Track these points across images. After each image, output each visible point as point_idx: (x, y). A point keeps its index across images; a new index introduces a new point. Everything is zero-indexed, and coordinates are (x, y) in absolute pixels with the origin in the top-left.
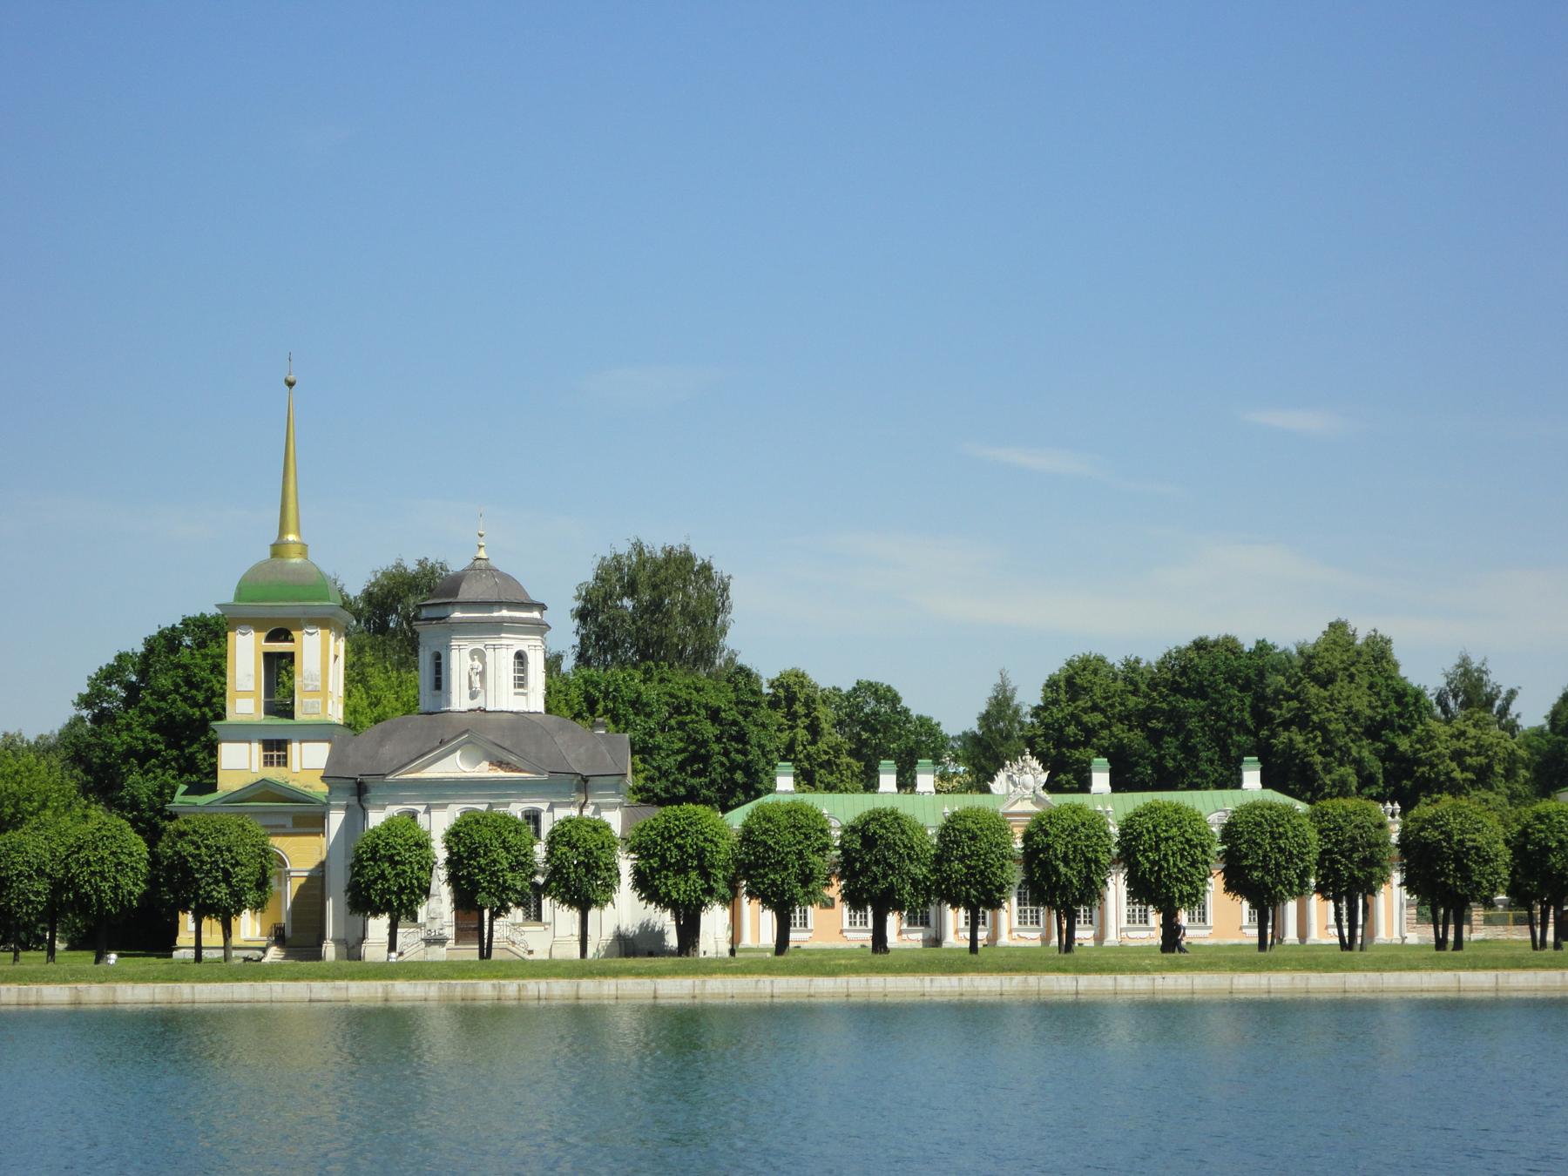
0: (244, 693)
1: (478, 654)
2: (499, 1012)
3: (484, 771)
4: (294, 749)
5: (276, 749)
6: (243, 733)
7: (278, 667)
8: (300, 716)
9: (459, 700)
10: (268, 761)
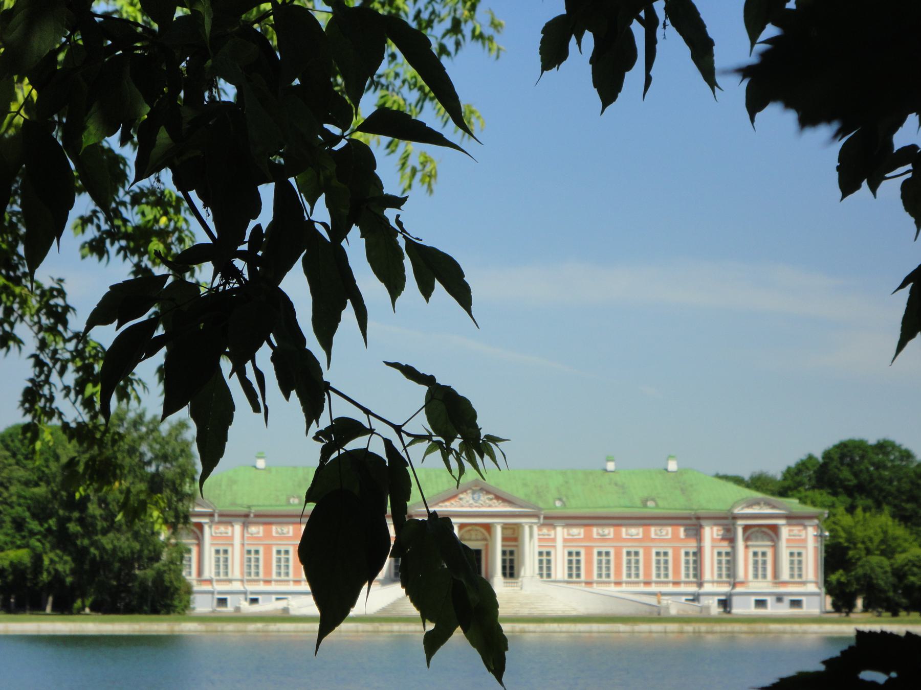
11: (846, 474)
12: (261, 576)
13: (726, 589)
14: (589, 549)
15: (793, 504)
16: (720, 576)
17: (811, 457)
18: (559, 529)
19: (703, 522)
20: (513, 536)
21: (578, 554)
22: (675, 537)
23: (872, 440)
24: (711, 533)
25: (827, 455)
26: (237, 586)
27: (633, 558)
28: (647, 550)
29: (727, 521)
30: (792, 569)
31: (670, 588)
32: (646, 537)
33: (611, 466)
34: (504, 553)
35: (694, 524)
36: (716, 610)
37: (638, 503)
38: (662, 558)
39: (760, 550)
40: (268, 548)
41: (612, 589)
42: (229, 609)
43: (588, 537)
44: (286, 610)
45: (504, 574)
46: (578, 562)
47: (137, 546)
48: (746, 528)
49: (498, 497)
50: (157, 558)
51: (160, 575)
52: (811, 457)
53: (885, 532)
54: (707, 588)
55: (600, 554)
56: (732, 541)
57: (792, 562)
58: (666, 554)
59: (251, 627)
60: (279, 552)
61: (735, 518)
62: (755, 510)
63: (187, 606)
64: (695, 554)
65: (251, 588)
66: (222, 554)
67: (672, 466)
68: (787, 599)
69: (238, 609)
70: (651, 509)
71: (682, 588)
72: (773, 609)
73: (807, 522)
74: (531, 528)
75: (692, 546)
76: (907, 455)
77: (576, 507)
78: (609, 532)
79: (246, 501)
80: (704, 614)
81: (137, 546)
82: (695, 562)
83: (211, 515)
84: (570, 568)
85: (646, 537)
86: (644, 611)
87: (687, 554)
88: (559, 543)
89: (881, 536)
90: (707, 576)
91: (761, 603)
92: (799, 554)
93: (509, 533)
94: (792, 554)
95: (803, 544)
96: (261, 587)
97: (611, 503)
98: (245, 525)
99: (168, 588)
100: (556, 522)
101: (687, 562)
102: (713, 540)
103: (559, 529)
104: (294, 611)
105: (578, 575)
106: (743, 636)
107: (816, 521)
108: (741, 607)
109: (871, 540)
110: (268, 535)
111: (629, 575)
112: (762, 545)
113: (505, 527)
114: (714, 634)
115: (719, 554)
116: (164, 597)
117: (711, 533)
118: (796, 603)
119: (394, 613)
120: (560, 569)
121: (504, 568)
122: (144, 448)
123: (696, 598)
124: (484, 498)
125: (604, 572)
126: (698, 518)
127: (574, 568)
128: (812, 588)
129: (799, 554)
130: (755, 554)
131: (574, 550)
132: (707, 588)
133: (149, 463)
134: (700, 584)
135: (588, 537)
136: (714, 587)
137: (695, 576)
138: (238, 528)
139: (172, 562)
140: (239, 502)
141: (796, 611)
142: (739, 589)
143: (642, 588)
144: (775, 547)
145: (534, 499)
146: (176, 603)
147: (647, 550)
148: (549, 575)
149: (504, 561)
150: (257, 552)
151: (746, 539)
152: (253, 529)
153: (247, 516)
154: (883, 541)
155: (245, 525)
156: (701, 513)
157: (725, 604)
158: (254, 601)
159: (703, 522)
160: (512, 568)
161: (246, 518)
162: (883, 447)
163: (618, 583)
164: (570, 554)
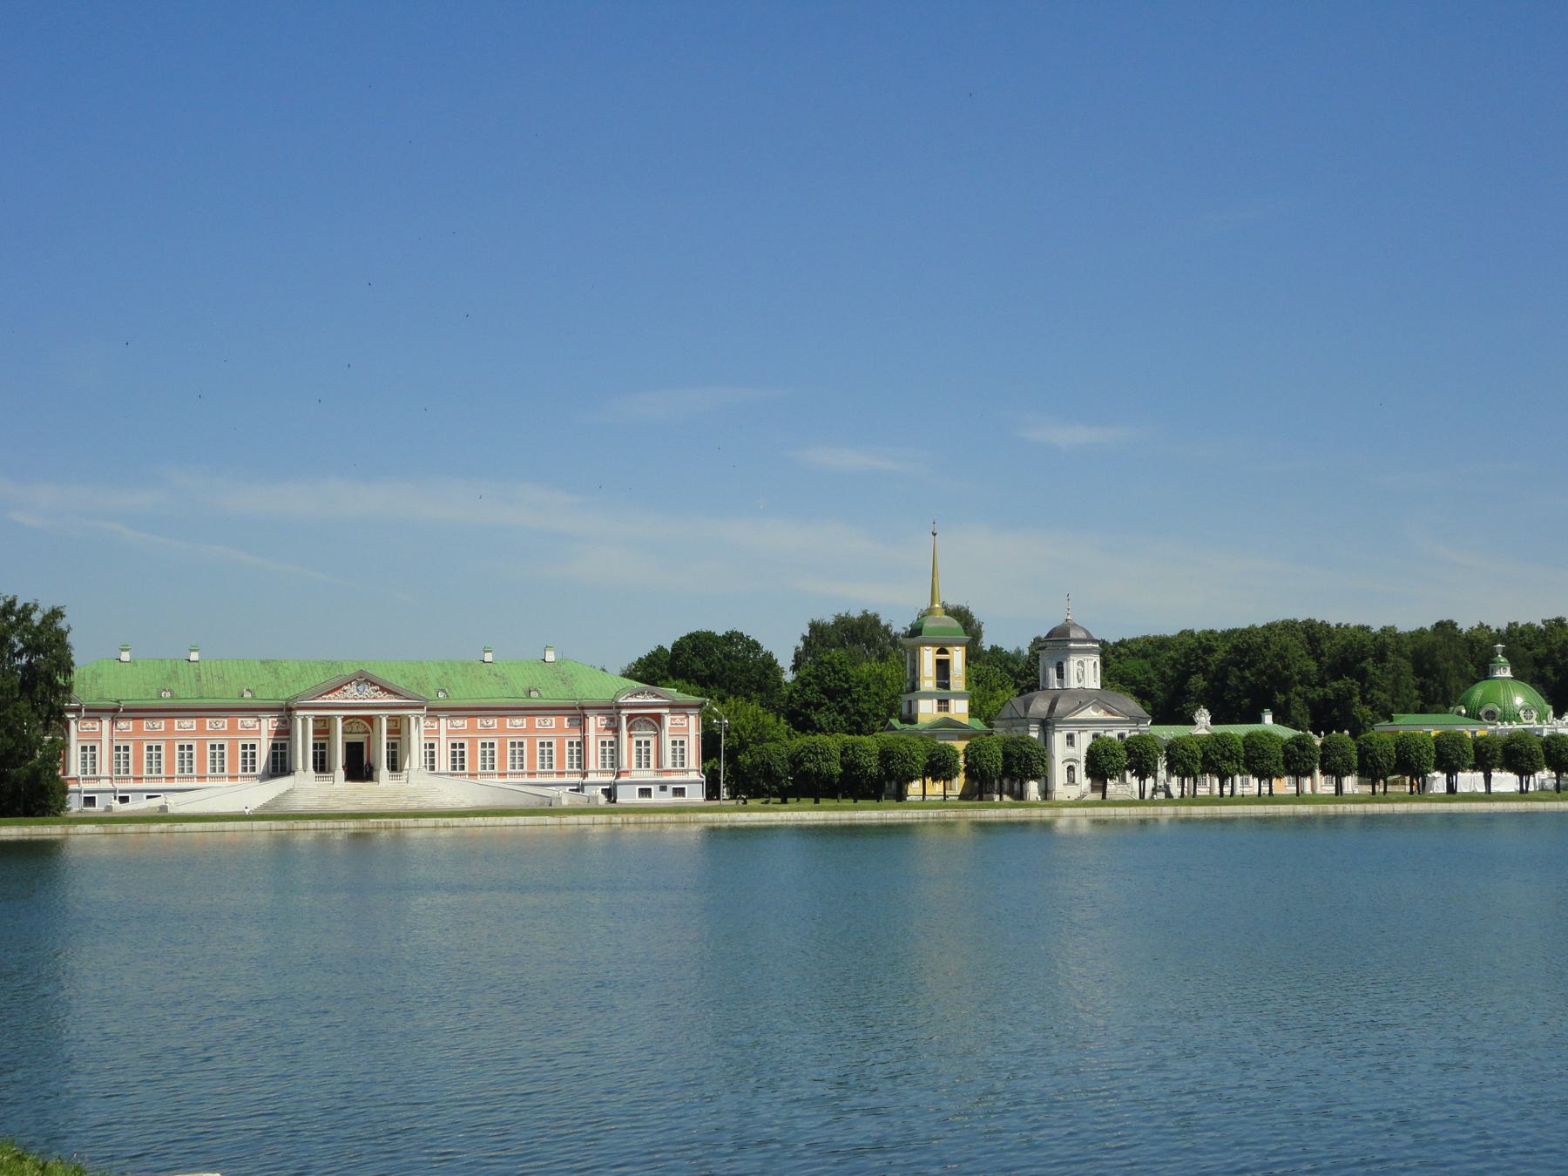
0: (928, 681)
1: (1081, 663)
2: (1336, 817)
3: (1100, 715)
4: (952, 702)
5: (943, 704)
6: (928, 695)
7: (943, 667)
8: (953, 689)
9: (1073, 683)
10: (940, 709)
11: (698, 664)
12: (131, 773)
13: (611, 778)
14: (473, 740)
15: (672, 693)
16: (604, 765)
17: (661, 648)
18: (442, 721)
19: (587, 712)
20: (398, 729)
21: (462, 745)
22: (560, 728)
23: (720, 633)
24: (595, 723)
25: (677, 647)
26: (105, 784)
27: (517, 749)
28: (532, 740)
29: (611, 711)
30: (674, 757)
31: (554, 779)
32: (531, 728)
33: (488, 657)
34: (315, 746)
35: (578, 714)
36: (603, 800)
37: (522, 694)
38: (546, 749)
39: (643, 739)
40: (138, 743)
41: (497, 780)
42: (99, 807)
43: (472, 729)
44: (163, 808)
45: (315, 768)
46: (462, 753)
47: (10, 742)
48: (630, 717)
49: (383, 689)
50: (32, 756)
51: (36, 773)
52: (661, 648)
53: (757, 720)
54: (592, 778)
55: (484, 745)
56: (616, 730)
57: (674, 751)
58: (550, 744)
59: (178, 827)
60: (150, 748)
61: (620, 707)
62: (640, 700)
63: (63, 805)
64: (578, 744)
65: (120, 786)
66: (89, 750)
67: (550, 656)
68: (670, 788)
69: (109, 809)
70: (534, 699)
71: (566, 779)
72: (658, 798)
73: (689, 711)
74: (417, 719)
75: (576, 736)
76: (754, 646)
77: (460, 697)
78: (493, 722)
79: (114, 695)
80: (592, 805)
81: (10, 742)
82: (579, 752)
83: (78, 710)
84: (454, 761)
85: (531, 728)
86: (534, 803)
87: (571, 744)
88: (443, 735)
89: (753, 724)
90: (591, 766)
91: (645, 792)
92: (682, 743)
93: (320, 726)
94: (674, 743)
95: (684, 731)
96: (131, 785)
97: (492, 693)
98: (114, 721)
99: (43, 788)
100: (440, 714)
101: (571, 752)
102: (597, 729)
103: (442, 721)
104: (174, 809)
105: (463, 768)
106: (671, 828)
107: (696, 711)
108: (628, 797)
109: (743, 728)
110: (138, 730)
111: (513, 767)
112: (646, 735)
113: (390, 719)
114: (597, 824)
115: (603, 743)
116: (40, 794)
117: (595, 723)
118: (679, 792)
119: (277, 810)
120: (444, 762)
121: (315, 762)
122: (15, 639)
123: (580, 788)
124: (369, 690)
125: (488, 764)
126: (582, 708)
127: (458, 759)
128: (694, 776)
129: (682, 743)
130: (639, 743)
131: (458, 742)
132: (592, 778)
133: (20, 655)
134: (585, 775)
135: (472, 729)
136: (599, 777)
137: (579, 766)
138: (106, 723)
139: (44, 759)
140: (107, 696)
141: (679, 799)
142: (623, 779)
143: (526, 779)
144: (658, 736)
145: (415, 690)
146: (51, 803)
147: (532, 740)
148: (432, 768)
149: (315, 754)
150: (126, 748)
151: (630, 729)
152: (122, 724)
153: (116, 710)
154: (755, 729)
155: (114, 721)
156: (585, 703)
157: (610, 793)
158: (124, 800)
159: (587, 712)
160: (323, 761)
161: (115, 713)
162: (732, 638)
163: (503, 775)
164: (454, 746)
